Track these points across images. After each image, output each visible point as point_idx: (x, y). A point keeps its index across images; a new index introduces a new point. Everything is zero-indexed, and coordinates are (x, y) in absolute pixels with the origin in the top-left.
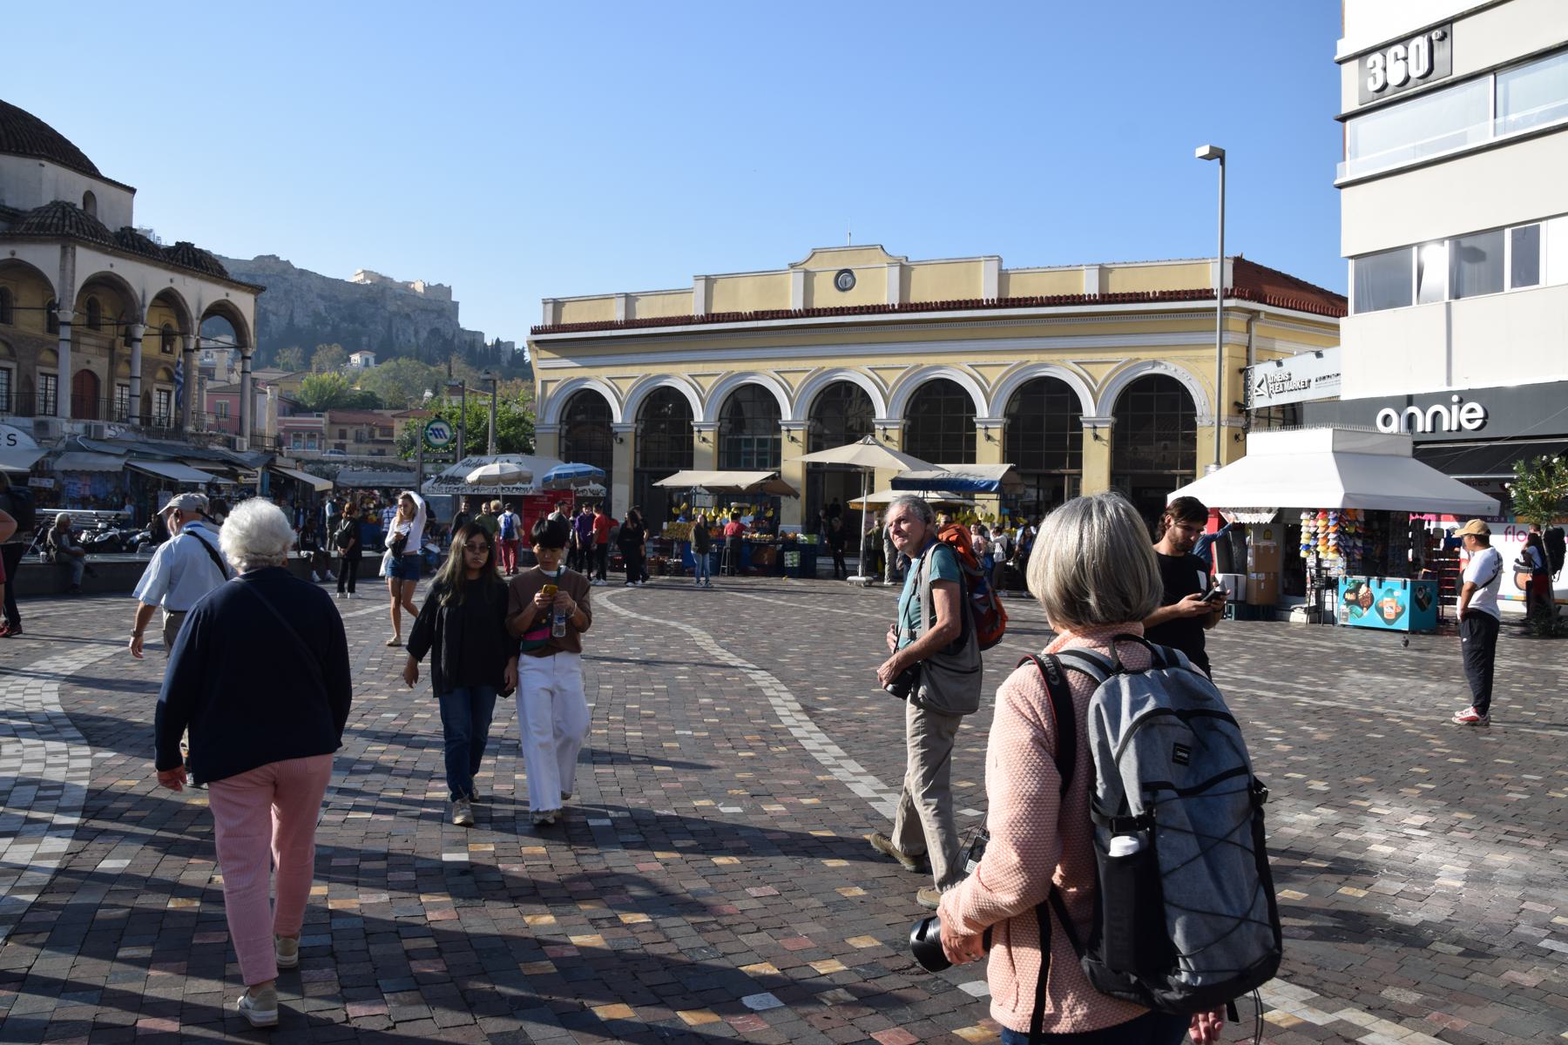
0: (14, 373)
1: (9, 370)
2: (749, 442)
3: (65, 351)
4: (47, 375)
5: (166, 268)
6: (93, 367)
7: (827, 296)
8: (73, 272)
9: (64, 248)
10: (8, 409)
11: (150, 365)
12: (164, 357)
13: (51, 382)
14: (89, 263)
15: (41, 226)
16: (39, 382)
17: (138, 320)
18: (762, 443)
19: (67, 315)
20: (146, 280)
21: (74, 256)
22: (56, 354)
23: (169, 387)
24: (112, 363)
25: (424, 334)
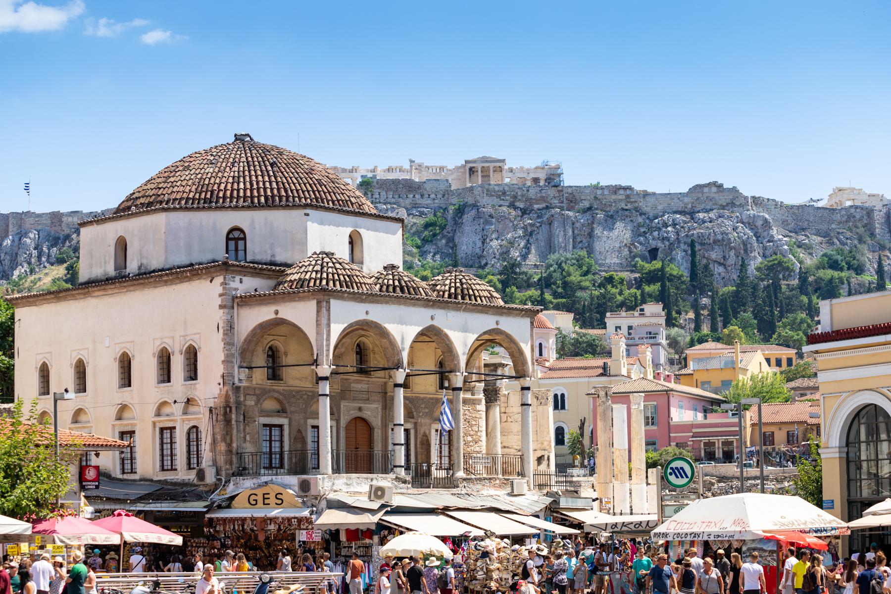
1: (281, 426)
4: (313, 427)
5: (426, 306)
6: (367, 414)
9: (319, 303)
10: (282, 466)
14: (344, 315)
15: (301, 282)
16: (310, 435)
17: (398, 366)
21: (329, 310)
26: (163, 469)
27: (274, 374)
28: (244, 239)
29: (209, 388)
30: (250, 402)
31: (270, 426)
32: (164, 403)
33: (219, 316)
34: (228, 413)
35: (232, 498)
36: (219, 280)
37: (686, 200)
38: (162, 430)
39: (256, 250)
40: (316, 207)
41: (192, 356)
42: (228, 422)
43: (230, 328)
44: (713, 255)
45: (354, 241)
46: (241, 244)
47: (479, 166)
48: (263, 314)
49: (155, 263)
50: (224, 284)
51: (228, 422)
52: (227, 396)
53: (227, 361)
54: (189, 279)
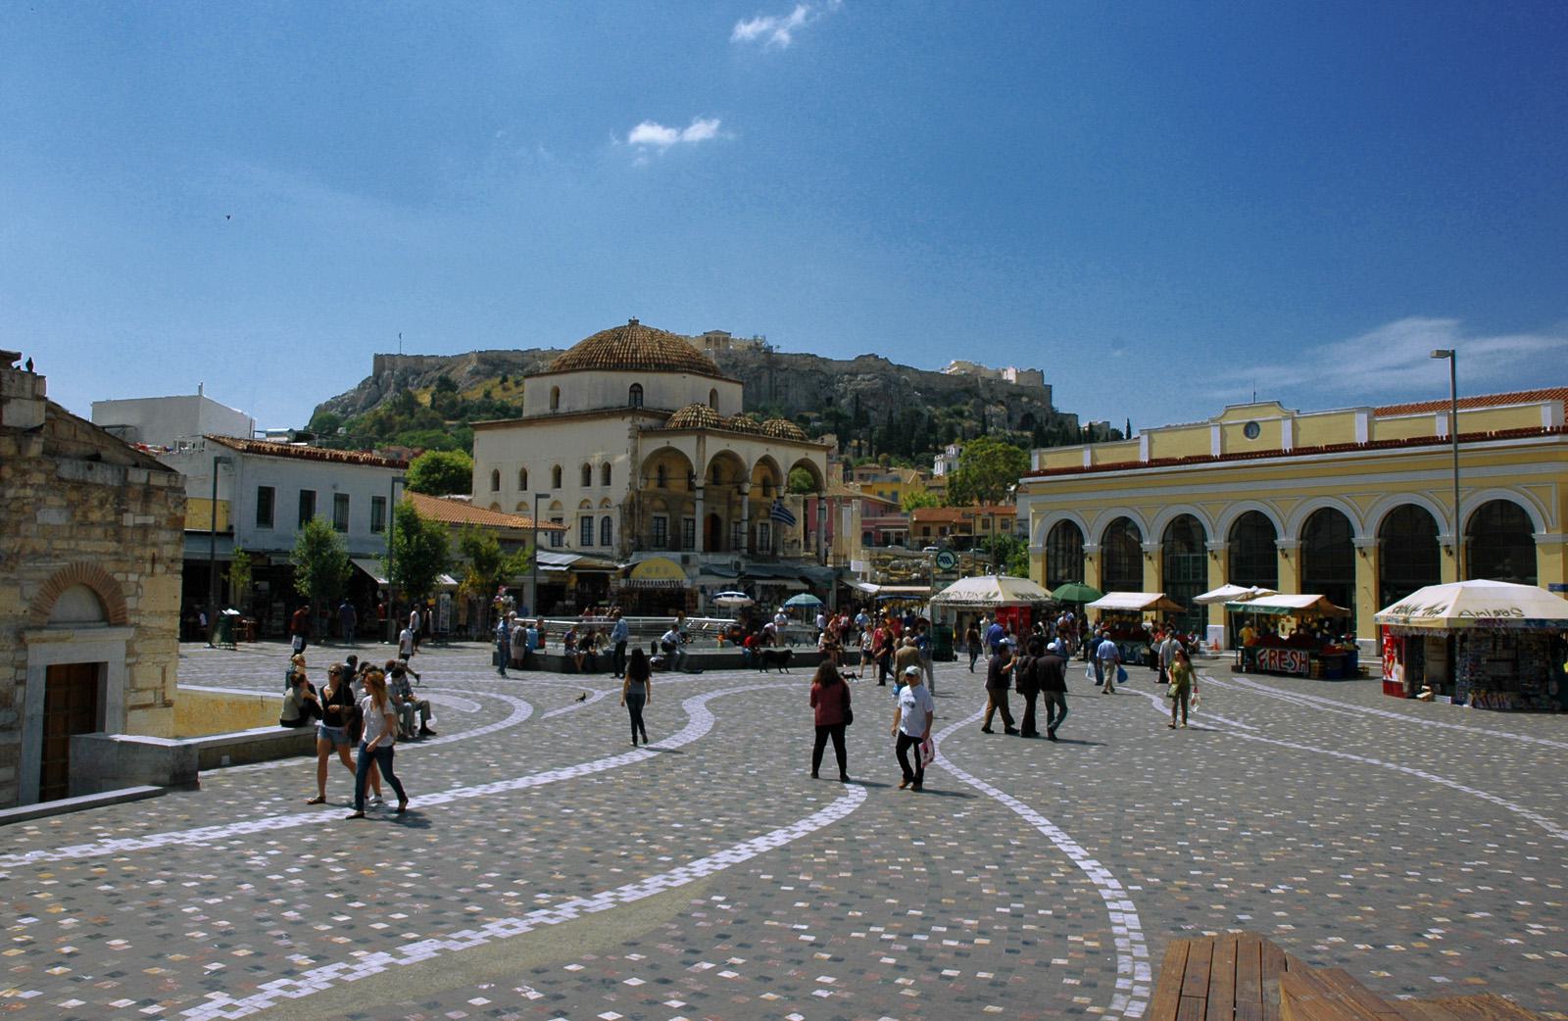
0: (668, 521)
1: (664, 519)
2: (1186, 559)
3: (700, 506)
4: (687, 520)
6: (718, 512)
7: (1240, 443)
8: (704, 452)
9: (699, 438)
10: (664, 545)
11: (754, 506)
12: (765, 500)
13: (691, 524)
14: (714, 445)
16: (683, 525)
17: (746, 480)
18: (1196, 559)
19: (700, 482)
20: (750, 452)
22: (695, 505)
23: (766, 521)
24: (729, 508)
25: (1017, 419)
26: (583, 544)
27: (661, 484)
28: (641, 392)
29: (620, 490)
30: (647, 502)
31: (657, 518)
32: (586, 500)
33: (627, 443)
34: (632, 509)
35: (634, 566)
36: (629, 419)
37: (853, 365)
38: (583, 518)
39: (650, 400)
40: (690, 373)
41: (607, 469)
42: (632, 514)
43: (635, 452)
44: (870, 404)
45: (714, 394)
46: (639, 395)
47: (712, 336)
48: (660, 443)
49: (582, 406)
50: (632, 422)
51: (632, 514)
52: (632, 498)
53: (633, 474)
54: (607, 417)
